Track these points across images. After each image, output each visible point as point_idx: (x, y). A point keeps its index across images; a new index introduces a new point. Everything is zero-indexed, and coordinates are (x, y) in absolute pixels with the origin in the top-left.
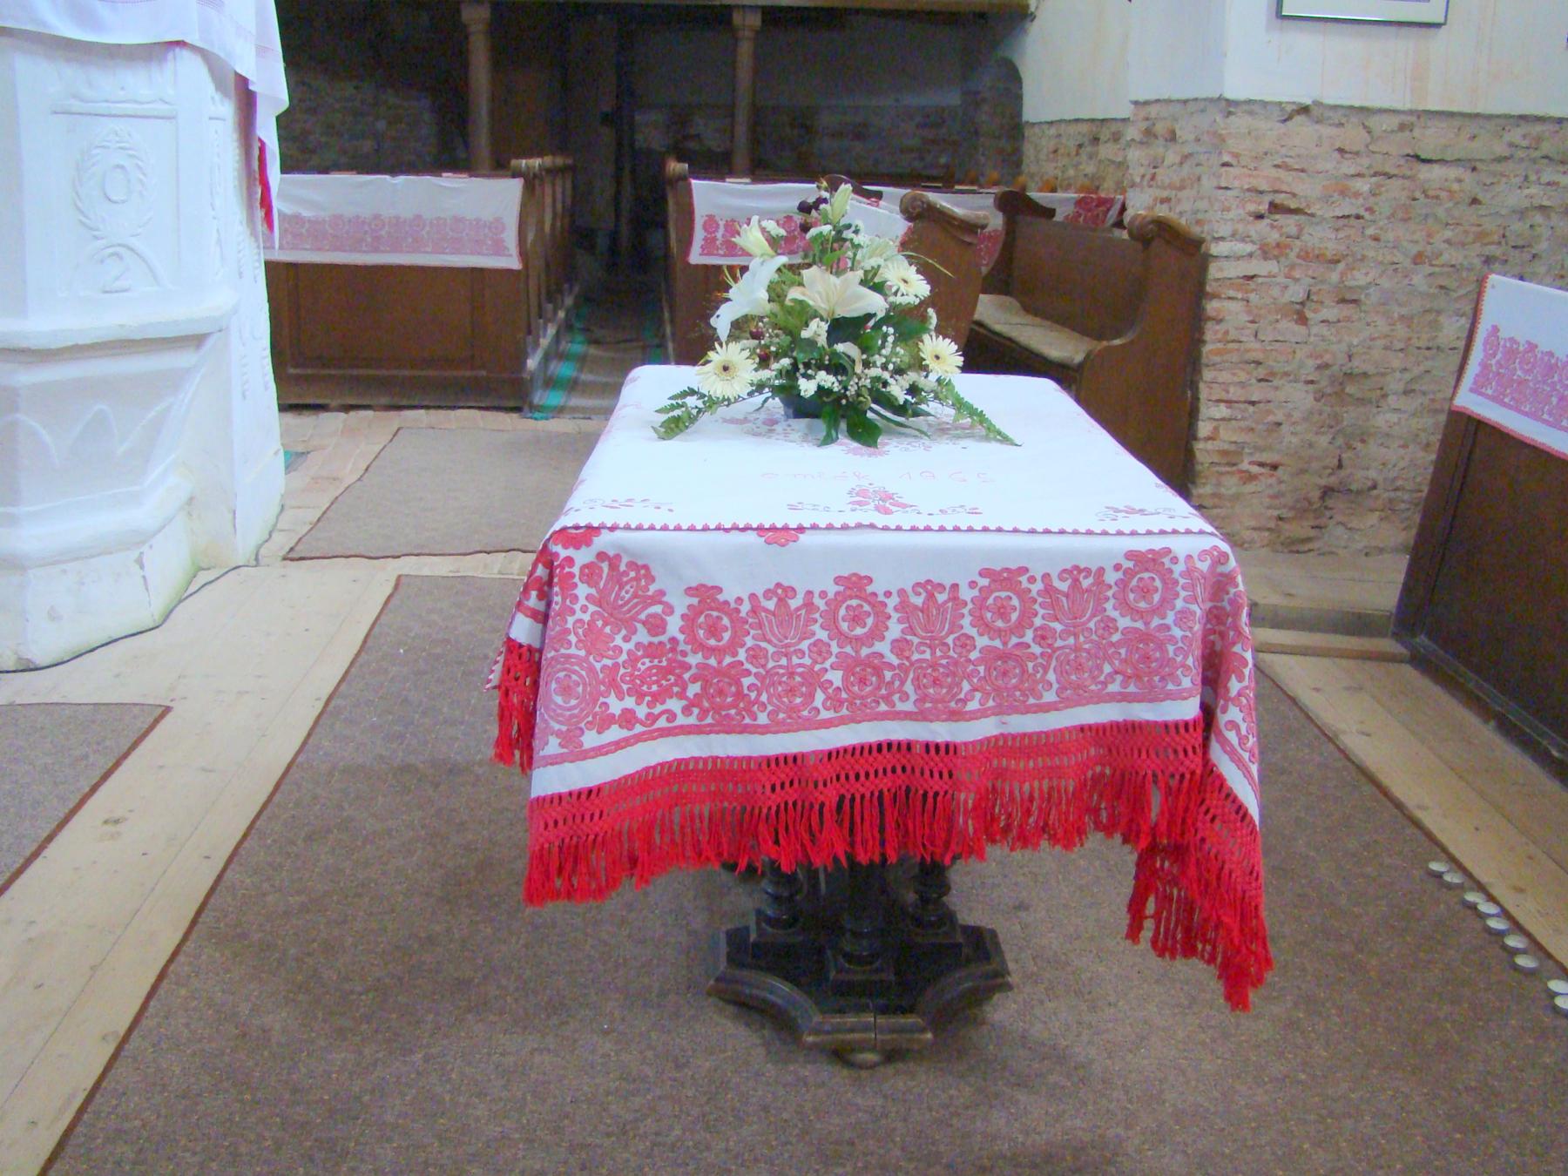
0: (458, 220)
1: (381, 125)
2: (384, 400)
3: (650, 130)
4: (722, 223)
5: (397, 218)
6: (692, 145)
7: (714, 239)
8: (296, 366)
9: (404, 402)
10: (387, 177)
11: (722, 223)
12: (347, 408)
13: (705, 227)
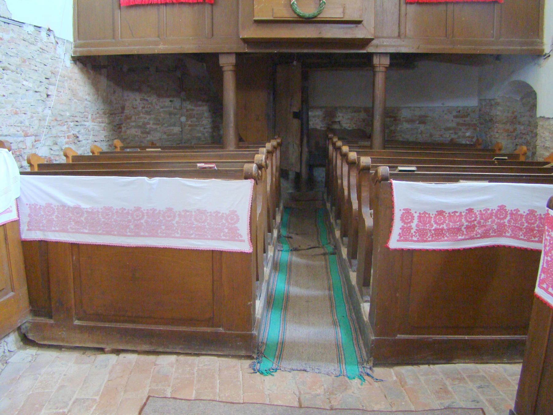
0: (201, 212)
2: (146, 347)
4: (416, 215)
5: (154, 210)
6: (336, 127)
7: (410, 228)
8: (79, 319)
9: (161, 350)
11: (416, 215)
12: (117, 352)
13: (402, 219)
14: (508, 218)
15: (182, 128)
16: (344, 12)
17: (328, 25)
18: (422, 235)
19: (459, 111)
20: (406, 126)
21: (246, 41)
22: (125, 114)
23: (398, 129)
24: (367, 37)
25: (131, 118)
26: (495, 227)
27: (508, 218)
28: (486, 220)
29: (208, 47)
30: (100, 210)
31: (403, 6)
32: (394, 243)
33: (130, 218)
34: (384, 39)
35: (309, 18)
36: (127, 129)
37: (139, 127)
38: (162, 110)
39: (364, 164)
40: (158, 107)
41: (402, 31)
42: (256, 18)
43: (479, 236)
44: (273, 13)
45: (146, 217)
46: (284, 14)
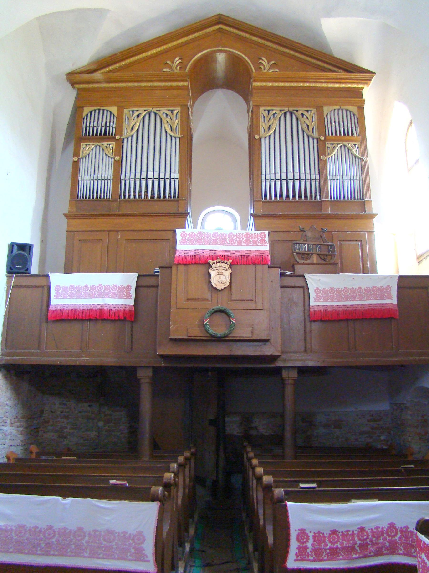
0: (110, 532)
1: (101, 424)
3: (233, 426)
4: (311, 535)
5: (65, 529)
7: (306, 548)
10: (60, 498)
11: (311, 535)
13: (298, 539)
14: (399, 535)
15: (99, 433)
16: (252, 332)
17: (238, 344)
18: (318, 555)
19: (372, 415)
20: (322, 430)
21: (162, 356)
22: (43, 418)
23: (315, 434)
24: (274, 354)
25: (48, 422)
26: (387, 544)
27: (399, 535)
28: (378, 538)
29: (128, 361)
30: (14, 528)
31: (308, 324)
32: (292, 563)
33: (42, 536)
34: (291, 354)
35: (219, 337)
36: (44, 432)
37: (57, 431)
38: (79, 414)
39: (266, 483)
40: (77, 412)
41: (308, 346)
42: (171, 337)
43: (372, 554)
44: (187, 332)
45: (57, 536)
46: (196, 332)
